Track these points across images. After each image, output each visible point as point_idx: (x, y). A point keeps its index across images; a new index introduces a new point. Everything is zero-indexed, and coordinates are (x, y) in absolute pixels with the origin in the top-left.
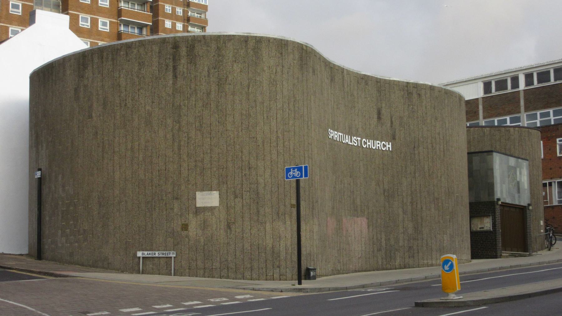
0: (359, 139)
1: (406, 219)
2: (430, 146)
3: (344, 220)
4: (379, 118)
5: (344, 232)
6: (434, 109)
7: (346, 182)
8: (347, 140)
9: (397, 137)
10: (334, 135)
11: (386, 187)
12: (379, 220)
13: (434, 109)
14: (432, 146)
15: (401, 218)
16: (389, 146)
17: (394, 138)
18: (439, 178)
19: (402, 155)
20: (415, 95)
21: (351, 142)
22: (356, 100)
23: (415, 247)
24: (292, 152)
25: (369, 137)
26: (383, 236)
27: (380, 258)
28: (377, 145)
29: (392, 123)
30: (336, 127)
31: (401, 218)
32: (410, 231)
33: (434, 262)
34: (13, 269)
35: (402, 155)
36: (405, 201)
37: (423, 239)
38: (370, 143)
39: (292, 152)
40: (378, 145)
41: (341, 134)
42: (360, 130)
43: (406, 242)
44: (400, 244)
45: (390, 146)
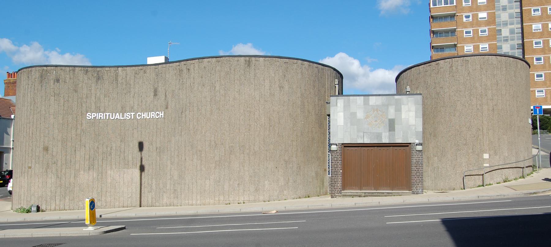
0: (133, 114)
1: (173, 168)
2: (195, 109)
3: (109, 172)
4: (155, 95)
5: (109, 181)
6: (202, 77)
7: (114, 145)
8: (118, 116)
9: (169, 107)
10: (90, 116)
11: (158, 145)
12: (151, 170)
13: (202, 77)
14: (198, 109)
15: (169, 168)
16: (162, 114)
17: (167, 108)
18: (204, 133)
19: (173, 119)
20: (185, 71)
21: (123, 116)
22: (132, 86)
23: (179, 190)
24: (31, 135)
25: (143, 111)
26: (154, 181)
27: (150, 197)
28: (152, 115)
29: (166, 96)
30: (102, 110)
31: (169, 168)
32: (176, 177)
33: (194, 202)
34: (539, 192)
35: (173, 119)
36: (173, 155)
37: (185, 184)
38: (145, 115)
39: (31, 135)
40: (153, 115)
41: (108, 114)
42: (136, 107)
43: (172, 186)
44: (168, 188)
45: (163, 114)
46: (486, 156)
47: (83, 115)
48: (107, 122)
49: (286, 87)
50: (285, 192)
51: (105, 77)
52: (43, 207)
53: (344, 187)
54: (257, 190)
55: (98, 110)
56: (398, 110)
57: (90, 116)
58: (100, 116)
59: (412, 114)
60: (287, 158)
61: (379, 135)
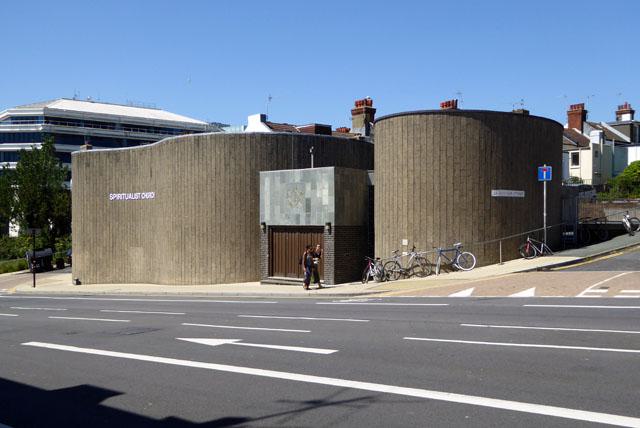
8: (130, 196)
46: (405, 242)
47: (107, 196)
48: (123, 202)
49: (233, 165)
50: (232, 275)
51: (122, 159)
52: (81, 281)
53: (271, 273)
54: (206, 272)
55: (118, 192)
56: (314, 187)
57: (112, 197)
58: (119, 196)
59: (326, 192)
60: (233, 240)
61: (298, 217)
